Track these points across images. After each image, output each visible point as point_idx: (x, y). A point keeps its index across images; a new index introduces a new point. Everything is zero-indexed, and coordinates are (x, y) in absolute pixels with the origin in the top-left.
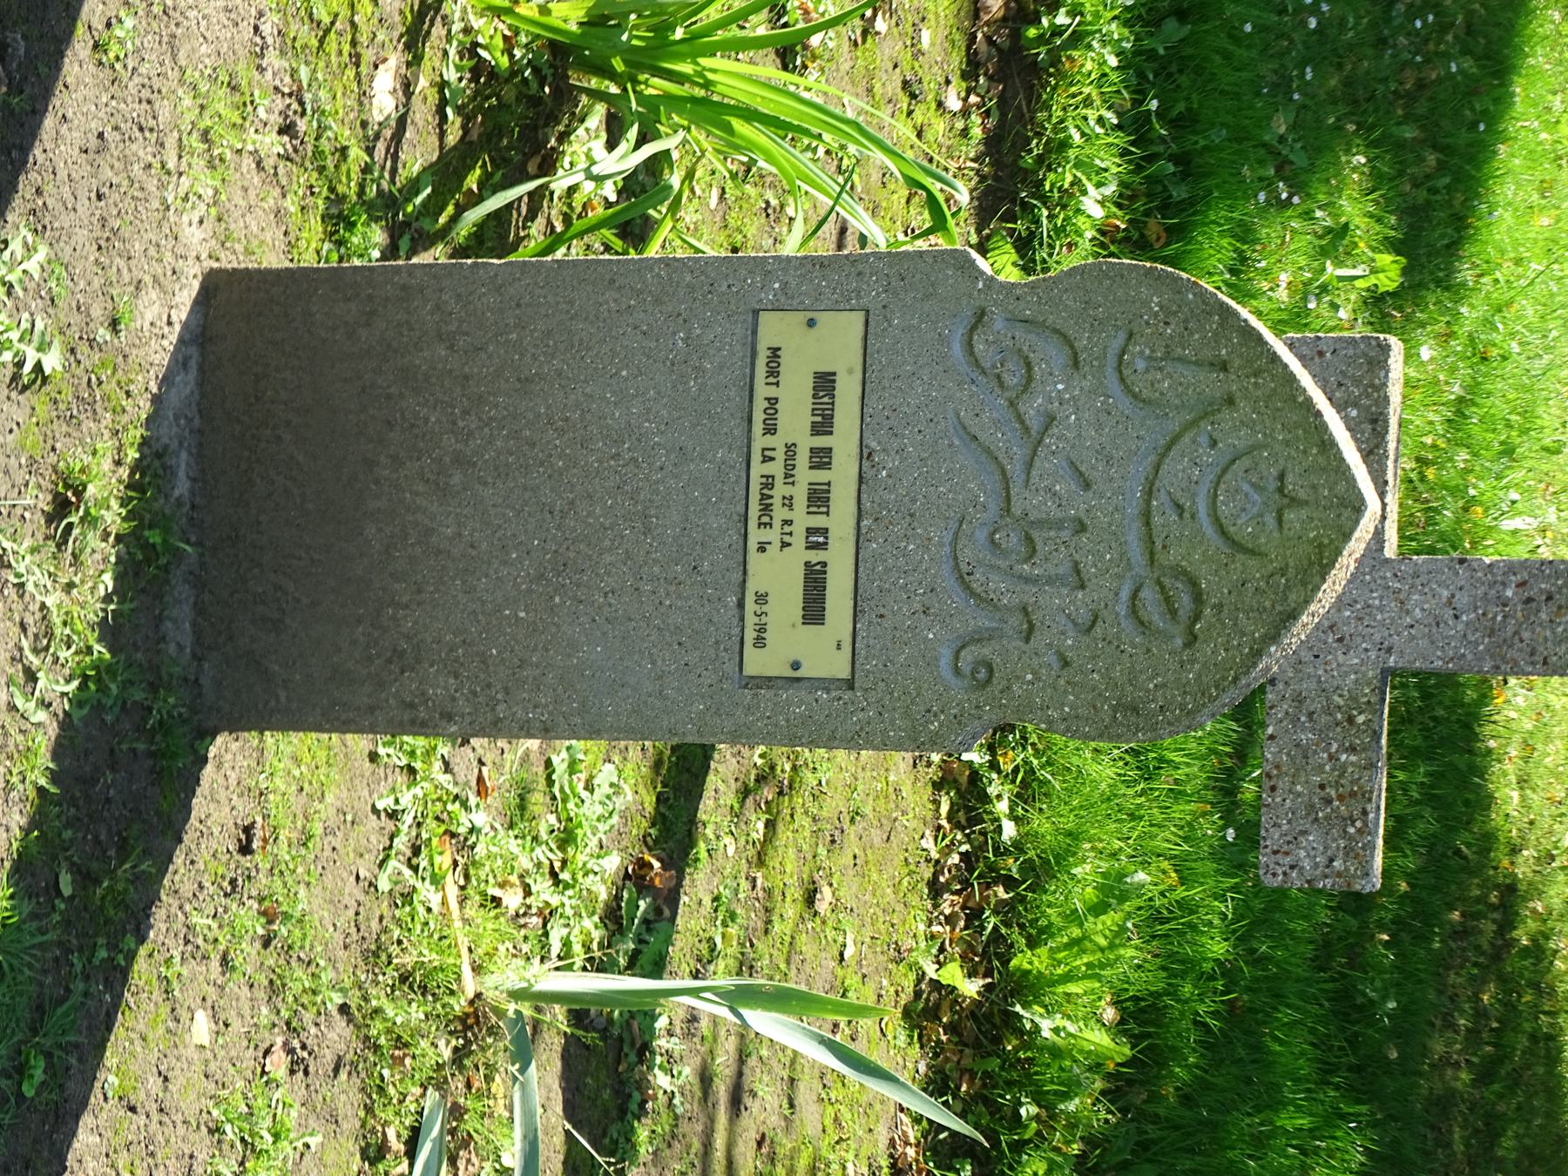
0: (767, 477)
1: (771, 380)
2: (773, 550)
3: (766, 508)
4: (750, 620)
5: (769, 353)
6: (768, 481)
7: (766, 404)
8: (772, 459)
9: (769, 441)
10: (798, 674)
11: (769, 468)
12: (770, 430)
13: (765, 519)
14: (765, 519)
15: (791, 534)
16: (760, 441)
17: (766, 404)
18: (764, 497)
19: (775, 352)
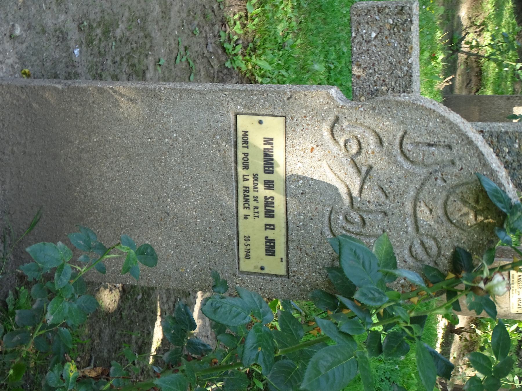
0: (246, 187)
1: (245, 145)
2: (250, 219)
3: (246, 201)
4: (242, 247)
5: (243, 133)
6: (247, 190)
7: (243, 156)
8: (248, 180)
9: (245, 172)
10: (263, 272)
11: (246, 184)
12: (246, 167)
13: (247, 205)
14: (247, 205)
15: (258, 212)
16: (241, 172)
17: (243, 156)
18: (245, 196)
19: (246, 133)
